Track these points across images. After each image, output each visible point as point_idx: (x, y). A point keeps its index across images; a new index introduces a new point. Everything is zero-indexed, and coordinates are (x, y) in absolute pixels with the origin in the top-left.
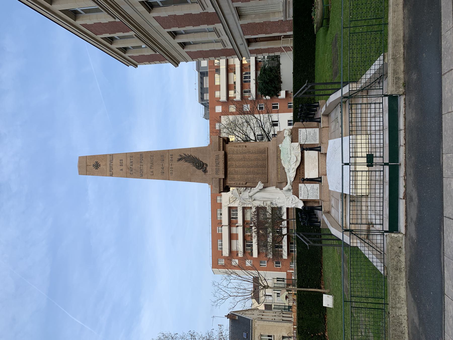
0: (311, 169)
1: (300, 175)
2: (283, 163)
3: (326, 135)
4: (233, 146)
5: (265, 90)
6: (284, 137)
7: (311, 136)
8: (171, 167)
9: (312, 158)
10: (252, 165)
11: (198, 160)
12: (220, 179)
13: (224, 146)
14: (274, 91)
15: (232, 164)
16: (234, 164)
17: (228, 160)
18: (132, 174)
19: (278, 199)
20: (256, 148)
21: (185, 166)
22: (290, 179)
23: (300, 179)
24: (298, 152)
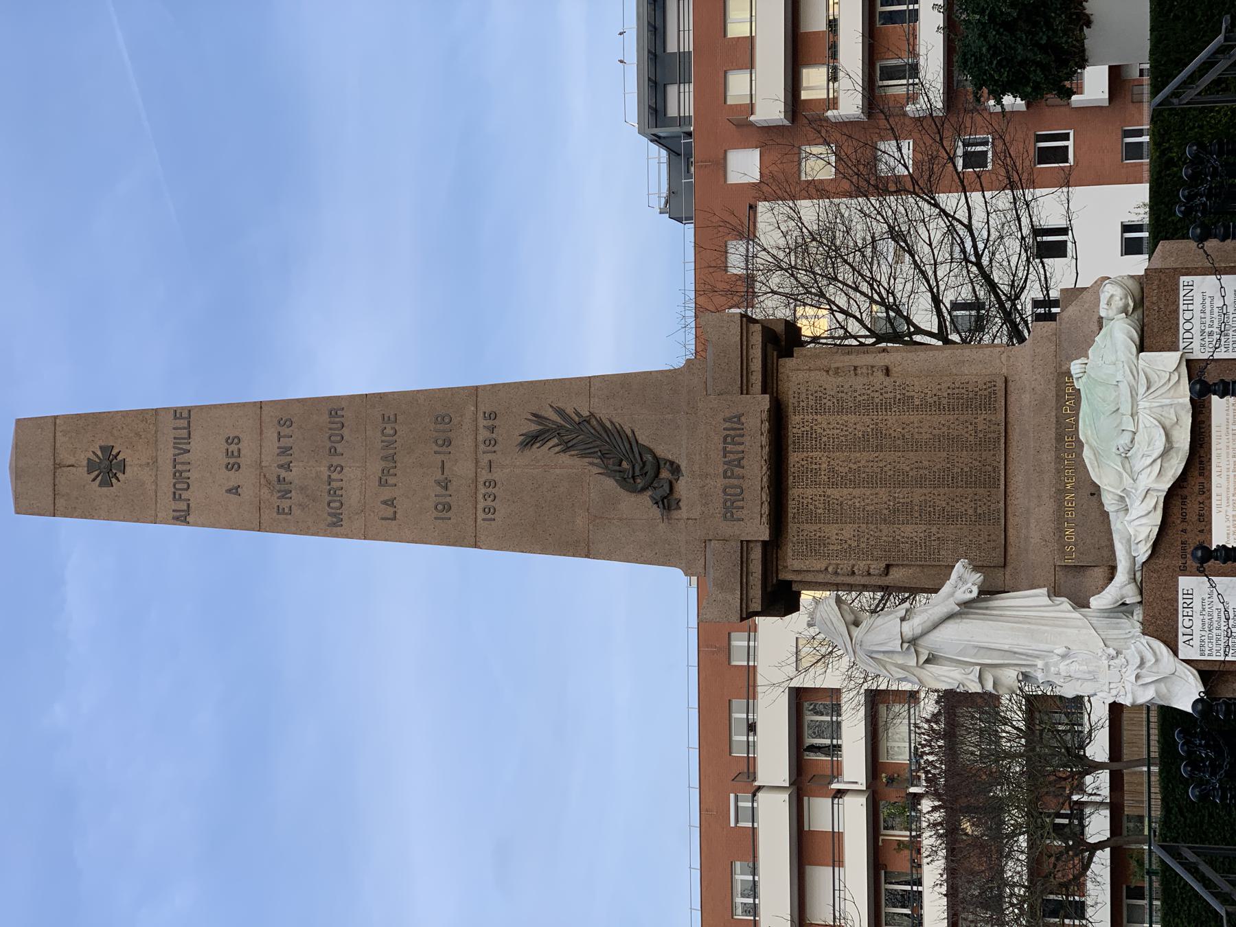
1: (1184, 531)
2: (1090, 463)
4: (820, 370)
5: (999, 63)
8: (490, 477)
10: (921, 472)
11: (631, 441)
12: (746, 545)
13: (769, 365)
15: (814, 466)
16: (824, 466)
17: (790, 442)
18: (286, 510)
19: (1064, 657)
20: (946, 378)
21: (558, 471)
23: (1184, 549)
24: (1176, 401)
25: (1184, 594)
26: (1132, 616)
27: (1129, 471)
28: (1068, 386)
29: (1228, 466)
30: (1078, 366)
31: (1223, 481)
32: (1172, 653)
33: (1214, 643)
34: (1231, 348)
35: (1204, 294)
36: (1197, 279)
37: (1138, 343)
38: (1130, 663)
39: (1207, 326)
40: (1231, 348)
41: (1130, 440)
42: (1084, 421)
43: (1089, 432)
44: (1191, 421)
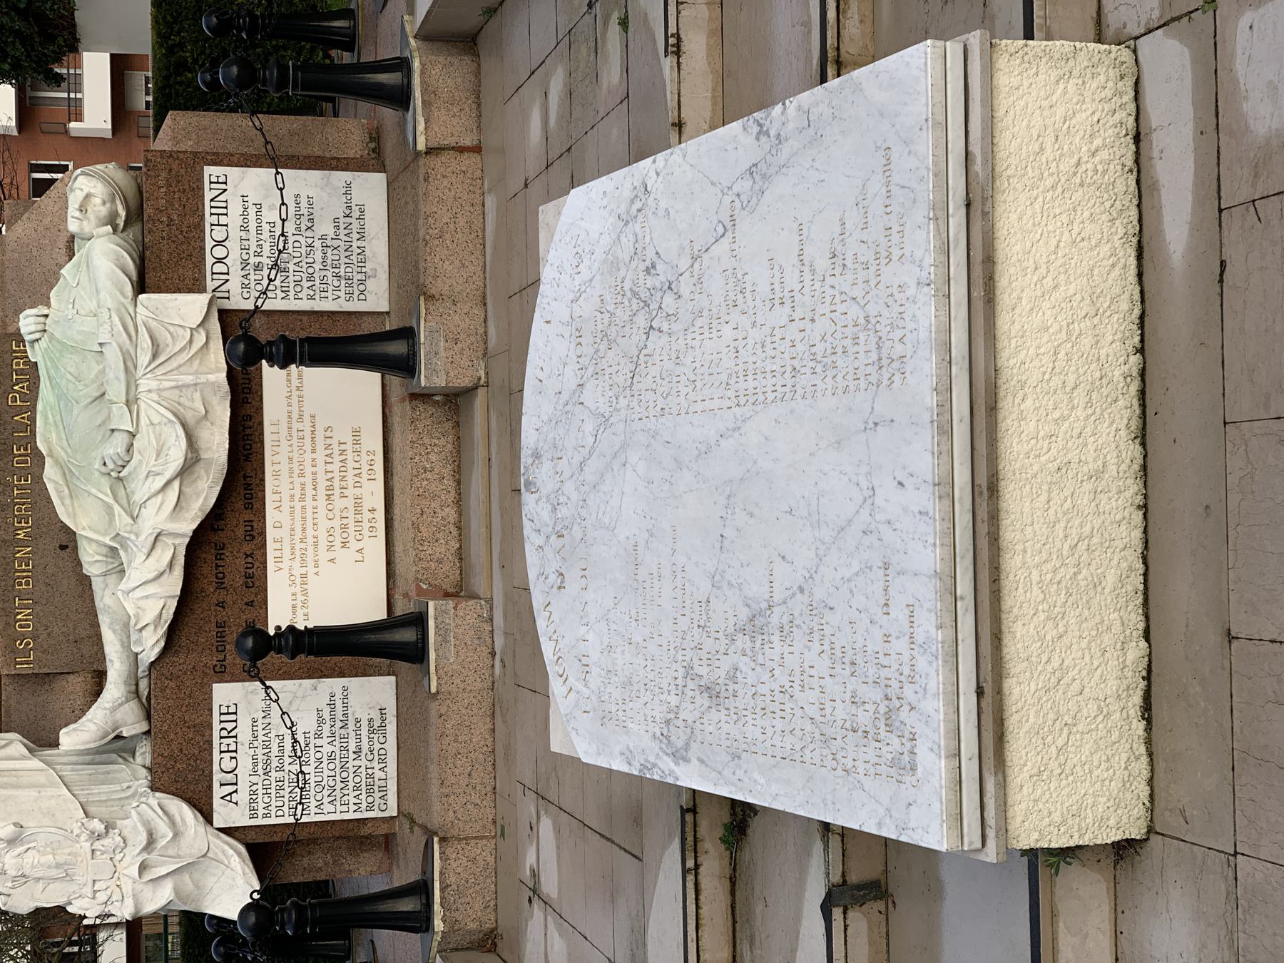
0: (323, 544)
1: (221, 604)
2: (59, 492)
3: (461, 222)
6: (72, 238)
7: (317, 244)
9: (334, 442)
14: (24, 39)
22: (126, 645)
23: (221, 636)
24: (203, 379)
25: (221, 714)
26: (134, 758)
27: (124, 502)
28: (17, 357)
29: (292, 492)
30: (32, 319)
31: (284, 517)
32: (201, 818)
33: (273, 796)
34: (292, 293)
35: (246, 199)
36: (233, 173)
37: (135, 278)
38: (129, 843)
39: (251, 252)
40: (292, 293)
41: (124, 447)
42: (46, 418)
43: (54, 435)
44: (229, 414)
